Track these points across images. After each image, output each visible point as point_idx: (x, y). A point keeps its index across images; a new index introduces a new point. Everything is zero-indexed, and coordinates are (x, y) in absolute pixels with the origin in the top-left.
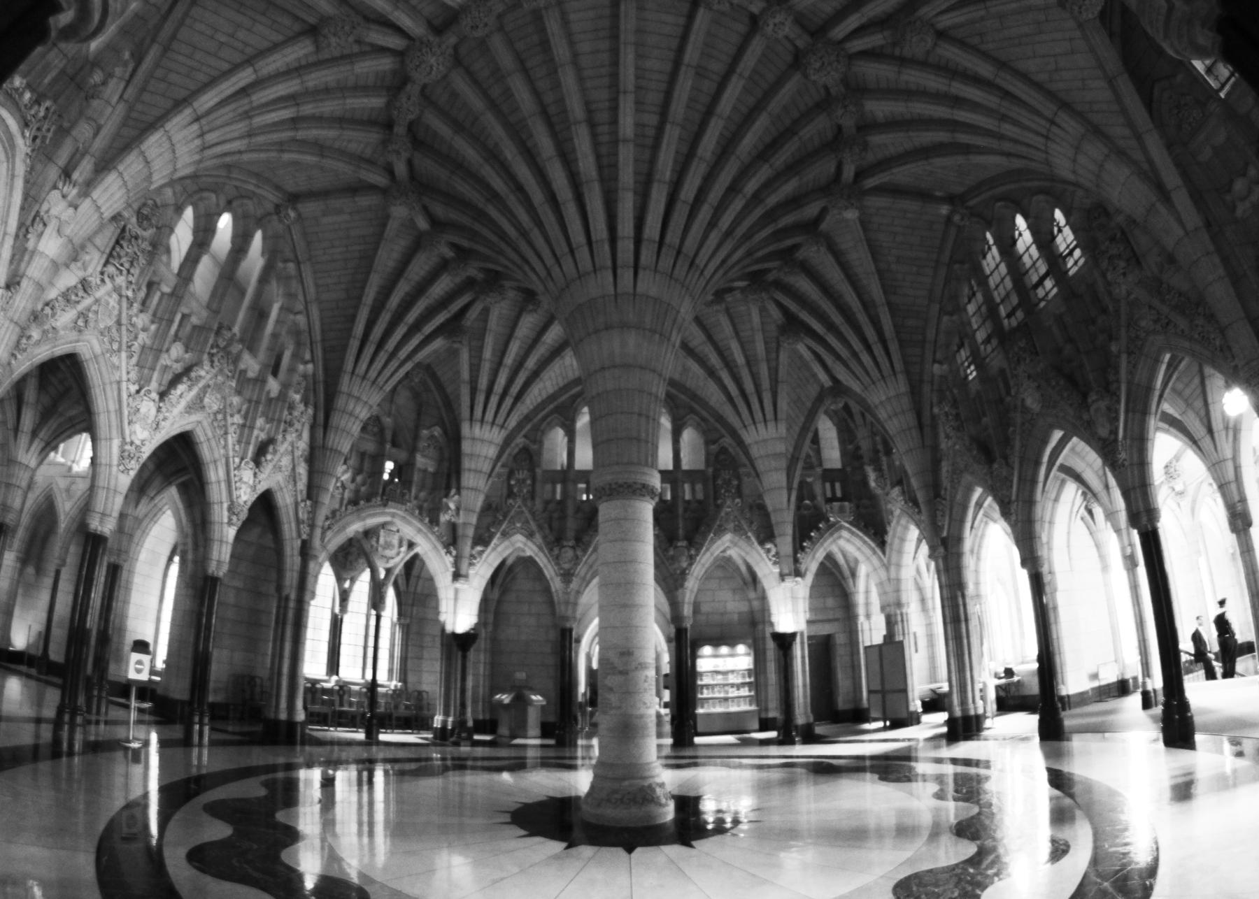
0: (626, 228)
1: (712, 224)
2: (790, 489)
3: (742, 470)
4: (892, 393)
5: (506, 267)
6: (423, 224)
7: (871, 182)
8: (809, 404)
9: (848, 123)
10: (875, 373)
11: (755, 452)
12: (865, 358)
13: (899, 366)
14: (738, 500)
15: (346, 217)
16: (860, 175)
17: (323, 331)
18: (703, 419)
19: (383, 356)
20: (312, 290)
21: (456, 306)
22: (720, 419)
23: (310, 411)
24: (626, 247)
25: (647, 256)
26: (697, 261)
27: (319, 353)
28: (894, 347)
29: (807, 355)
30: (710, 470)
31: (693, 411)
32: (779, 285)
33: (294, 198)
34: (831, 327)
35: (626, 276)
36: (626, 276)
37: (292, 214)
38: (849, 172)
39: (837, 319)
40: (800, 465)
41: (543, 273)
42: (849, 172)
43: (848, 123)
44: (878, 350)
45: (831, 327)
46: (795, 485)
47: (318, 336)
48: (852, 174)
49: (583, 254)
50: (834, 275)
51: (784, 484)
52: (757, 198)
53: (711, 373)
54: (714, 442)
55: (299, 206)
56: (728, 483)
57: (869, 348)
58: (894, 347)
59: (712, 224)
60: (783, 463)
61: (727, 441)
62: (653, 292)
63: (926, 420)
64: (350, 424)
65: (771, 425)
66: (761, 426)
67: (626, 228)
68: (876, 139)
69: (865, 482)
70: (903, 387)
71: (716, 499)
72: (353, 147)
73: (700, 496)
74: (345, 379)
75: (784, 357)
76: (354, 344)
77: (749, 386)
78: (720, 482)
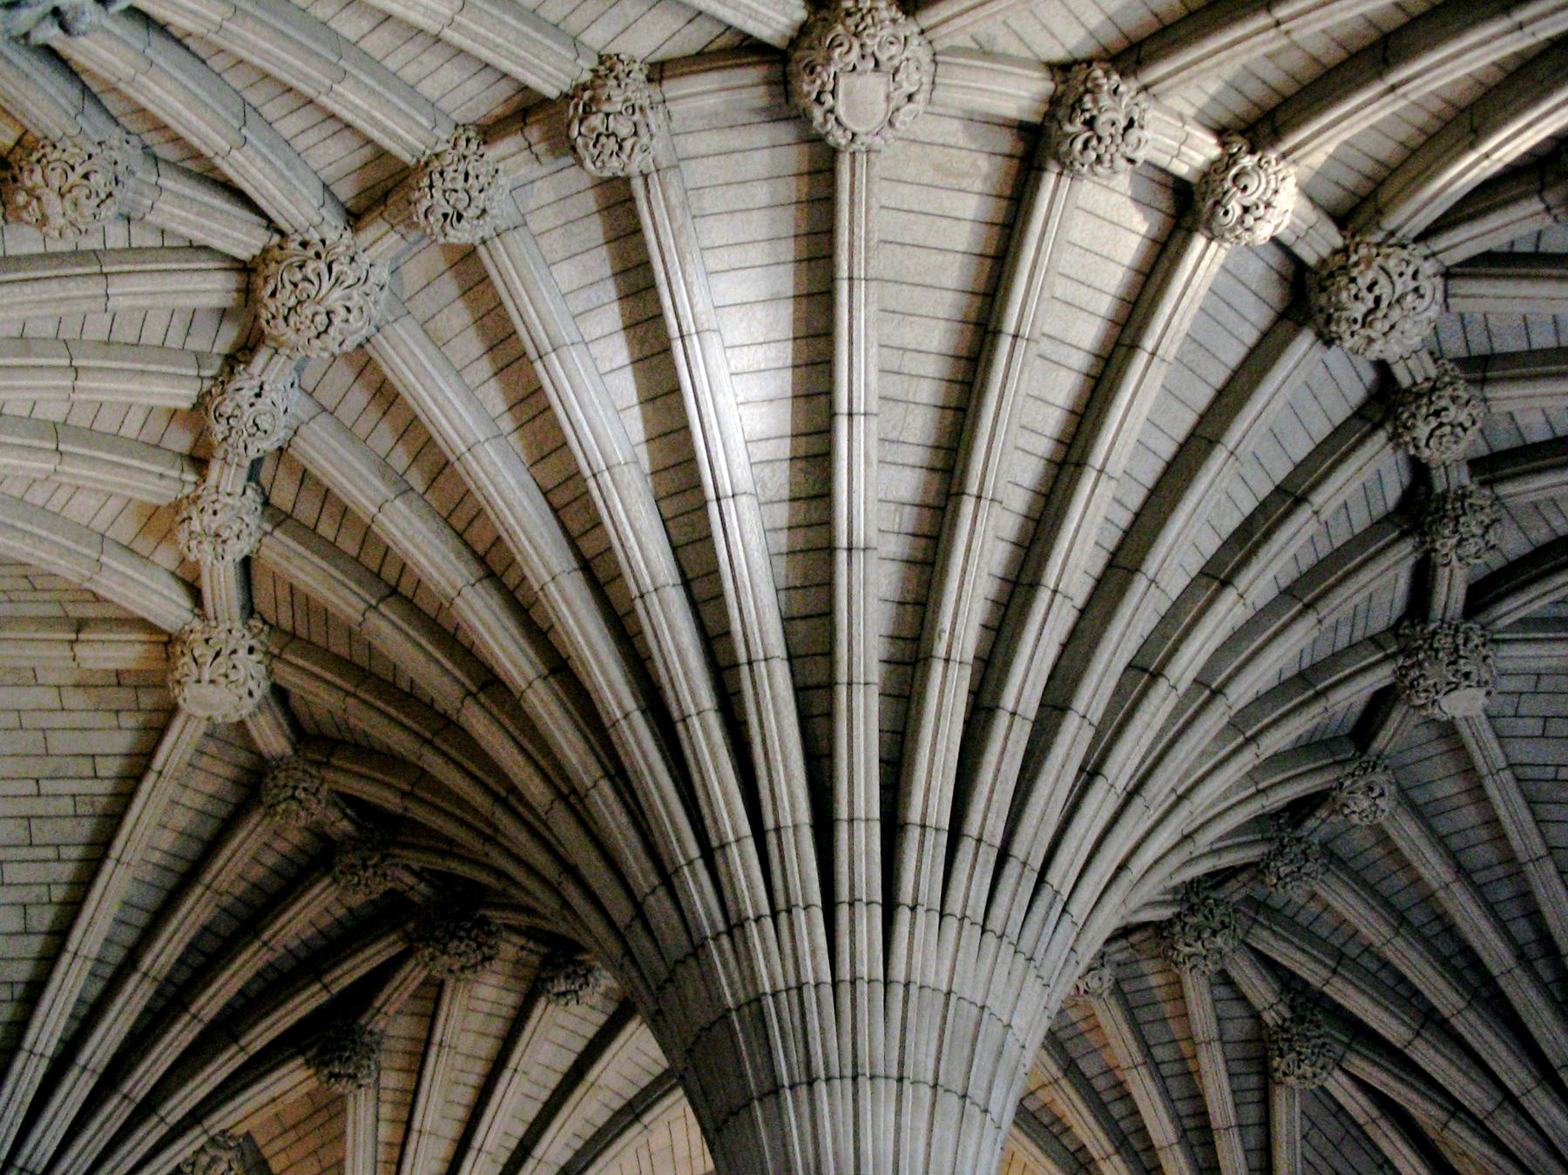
0: (860, 790)
1: (1090, 773)
5: (501, 874)
6: (272, 738)
7: (1512, 609)
9: (1449, 457)
15: (49, 698)
16: (1483, 595)
19: (115, 1112)
21: (347, 974)
24: (861, 844)
26: (1054, 877)
29: (1358, 1106)
34: (1431, 1020)
38: (1450, 592)
39: (1444, 996)
41: (622, 912)
42: (1450, 592)
43: (1449, 457)
45: (1431, 1020)
48: (1459, 592)
49: (743, 861)
52: (1208, 688)
59: (1090, 773)
67: (860, 790)
68: (1521, 491)
75: (1287, 1114)
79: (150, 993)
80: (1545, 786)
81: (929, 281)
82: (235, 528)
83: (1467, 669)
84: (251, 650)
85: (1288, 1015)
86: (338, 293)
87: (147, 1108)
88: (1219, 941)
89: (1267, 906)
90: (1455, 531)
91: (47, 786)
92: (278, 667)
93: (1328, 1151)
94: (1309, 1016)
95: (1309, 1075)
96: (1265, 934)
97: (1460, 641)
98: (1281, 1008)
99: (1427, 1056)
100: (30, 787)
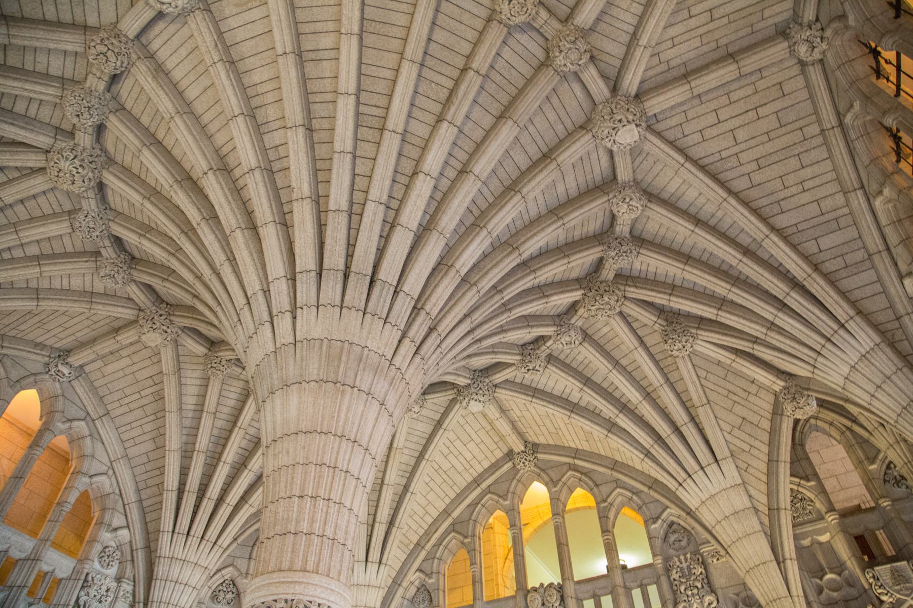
2: (780, 562)
3: (705, 549)
4: (854, 357)
8: (766, 425)
10: (814, 339)
11: (707, 517)
12: (785, 321)
13: (842, 310)
14: (709, 598)
17: (138, 491)
18: (636, 493)
19: (207, 506)
20: (115, 448)
22: (654, 484)
23: (127, 587)
25: (306, 290)
27: (135, 515)
28: (818, 286)
29: (724, 357)
30: (659, 560)
31: (618, 484)
32: (624, 278)
33: (64, 354)
34: (723, 303)
35: (284, 323)
36: (284, 323)
37: (65, 370)
39: (720, 288)
40: (786, 519)
44: (795, 300)
45: (723, 303)
46: (789, 548)
47: (131, 495)
50: (681, 231)
51: (768, 554)
53: (611, 427)
54: (655, 520)
55: (70, 360)
56: (687, 574)
57: (783, 306)
58: (818, 286)
60: (753, 523)
61: (672, 513)
62: (317, 333)
64: (177, 595)
65: (712, 470)
66: (699, 476)
70: (866, 338)
72: (76, 283)
74: (165, 538)
75: (686, 370)
76: (170, 499)
77: (663, 429)
78: (675, 575)
79: (204, 458)
80: (718, 164)
81: (254, 52)
82: (116, 269)
83: (619, 118)
84: (161, 315)
85: (664, 323)
86: (68, 163)
87: (220, 500)
88: (606, 298)
90: (561, 51)
91: (143, 393)
92: (172, 318)
93: (721, 382)
94: (675, 321)
95: (681, 347)
96: (632, 289)
97: (613, 106)
98: (659, 321)
100: (137, 396)
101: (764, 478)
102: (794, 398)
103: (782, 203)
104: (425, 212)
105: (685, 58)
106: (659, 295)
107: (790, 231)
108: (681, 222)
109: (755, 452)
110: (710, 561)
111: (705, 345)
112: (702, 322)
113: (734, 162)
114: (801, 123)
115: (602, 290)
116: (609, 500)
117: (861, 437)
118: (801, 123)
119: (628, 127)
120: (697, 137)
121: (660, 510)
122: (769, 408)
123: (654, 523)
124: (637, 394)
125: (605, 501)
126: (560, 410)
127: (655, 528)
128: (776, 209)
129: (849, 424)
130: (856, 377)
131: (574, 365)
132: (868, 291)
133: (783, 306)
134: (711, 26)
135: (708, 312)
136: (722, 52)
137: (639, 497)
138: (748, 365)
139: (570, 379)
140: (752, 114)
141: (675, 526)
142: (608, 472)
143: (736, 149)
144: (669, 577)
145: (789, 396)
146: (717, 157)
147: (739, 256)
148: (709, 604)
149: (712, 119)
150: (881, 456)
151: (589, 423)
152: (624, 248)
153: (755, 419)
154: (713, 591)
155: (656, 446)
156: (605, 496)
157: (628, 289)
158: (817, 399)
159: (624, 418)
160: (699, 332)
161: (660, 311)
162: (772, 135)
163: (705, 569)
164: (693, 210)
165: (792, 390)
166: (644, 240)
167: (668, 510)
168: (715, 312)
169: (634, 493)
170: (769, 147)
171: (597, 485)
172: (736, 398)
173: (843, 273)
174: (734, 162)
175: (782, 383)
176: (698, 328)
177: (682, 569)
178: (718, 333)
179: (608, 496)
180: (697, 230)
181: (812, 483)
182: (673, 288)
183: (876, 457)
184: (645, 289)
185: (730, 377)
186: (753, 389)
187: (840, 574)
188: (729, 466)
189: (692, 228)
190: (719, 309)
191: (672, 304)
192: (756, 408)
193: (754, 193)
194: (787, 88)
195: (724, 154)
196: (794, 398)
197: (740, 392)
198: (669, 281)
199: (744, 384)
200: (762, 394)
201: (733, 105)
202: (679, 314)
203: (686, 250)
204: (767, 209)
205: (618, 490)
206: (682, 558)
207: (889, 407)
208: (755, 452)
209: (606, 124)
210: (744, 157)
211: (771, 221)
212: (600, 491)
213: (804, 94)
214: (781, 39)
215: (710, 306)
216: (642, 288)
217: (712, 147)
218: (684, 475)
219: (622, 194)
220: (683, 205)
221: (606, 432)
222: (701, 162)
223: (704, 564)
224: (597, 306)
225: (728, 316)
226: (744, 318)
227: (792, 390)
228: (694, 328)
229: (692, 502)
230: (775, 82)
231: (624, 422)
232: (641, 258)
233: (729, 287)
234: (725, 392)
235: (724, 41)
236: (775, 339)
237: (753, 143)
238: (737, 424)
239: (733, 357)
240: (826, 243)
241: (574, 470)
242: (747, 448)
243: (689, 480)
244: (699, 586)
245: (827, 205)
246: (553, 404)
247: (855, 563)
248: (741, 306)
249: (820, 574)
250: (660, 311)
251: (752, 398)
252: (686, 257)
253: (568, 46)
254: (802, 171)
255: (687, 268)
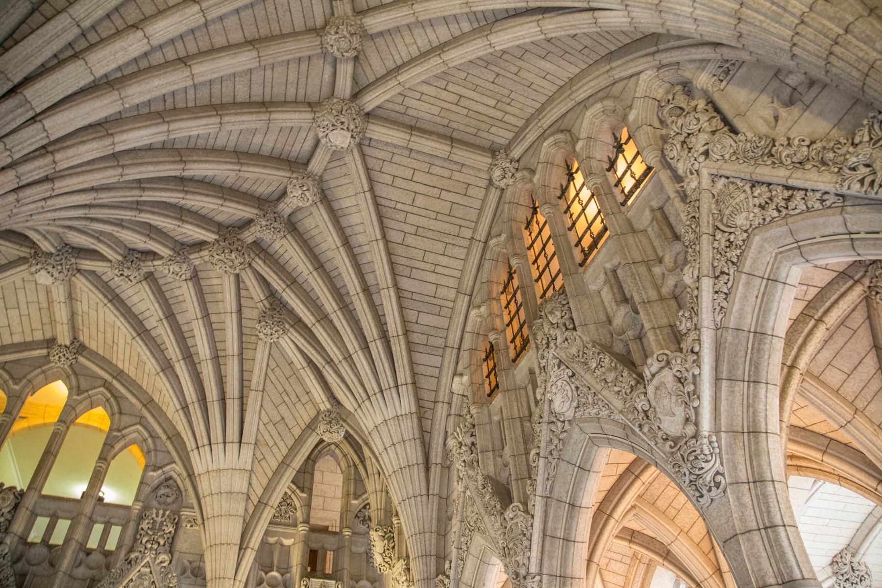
3: (185, 513)
4: (391, 414)
8: (297, 432)
10: (371, 385)
11: (204, 486)
13: (404, 375)
14: (164, 557)
18: (154, 436)
22: (175, 437)
28: (399, 347)
29: (298, 361)
30: (138, 506)
31: (142, 421)
32: (259, 248)
34: (324, 318)
39: (330, 305)
40: (267, 515)
44: (377, 348)
46: (255, 541)
50: (328, 241)
53: (167, 367)
54: (156, 468)
56: (156, 528)
57: (365, 347)
58: (399, 347)
60: (239, 507)
61: (176, 469)
63: (436, 457)
65: (232, 448)
66: (218, 449)
69: (369, 555)
70: (406, 404)
71: (131, 551)
73: (111, 545)
75: (261, 355)
78: (145, 525)
80: (390, 210)
83: (343, 120)
85: (268, 306)
88: (233, 256)
89: (266, 252)
94: (278, 309)
95: (269, 332)
96: (260, 262)
97: (345, 108)
98: (265, 302)
99: (320, 332)
101: (270, 474)
102: (330, 422)
103: (414, 270)
104: (120, 68)
105: (421, 115)
106: (278, 281)
107: (406, 294)
108: (334, 234)
109: (275, 450)
110: (184, 524)
111: (289, 343)
112: (298, 323)
113: (401, 216)
114: (463, 223)
115: (235, 246)
116: (124, 432)
117: (360, 476)
118: (463, 223)
119: (345, 133)
120: (388, 179)
121: (166, 461)
122: (307, 420)
123: (154, 470)
124: (208, 352)
125: (119, 431)
126: (128, 326)
127: (152, 476)
128: (406, 272)
129: (357, 461)
130: (383, 429)
131: (168, 295)
132: (429, 371)
133: (365, 347)
134: (453, 108)
135: (308, 318)
136: (447, 132)
137: (154, 442)
138: (312, 377)
139: (157, 305)
140: (436, 192)
141: (171, 482)
142: (138, 405)
143: (409, 209)
144: (139, 524)
145: (328, 419)
146: (392, 204)
147: (359, 290)
148: (161, 562)
149: (408, 174)
150: (364, 497)
151: (148, 353)
152: (276, 225)
153: (291, 423)
154: (171, 552)
155: (196, 405)
156: (121, 427)
157: (257, 259)
158: (347, 432)
159: (183, 366)
160: (291, 330)
161: (272, 294)
162: (440, 217)
163: (176, 530)
164: (348, 231)
165: (333, 416)
166: (296, 229)
167: (174, 465)
168: (314, 321)
169: (151, 436)
170: (432, 224)
171: (120, 413)
172: (286, 399)
173: (421, 348)
174: (401, 216)
175: (329, 406)
176: (292, 326)
177: (155, 522)
178: (305, 339)
179: (125, 428)
180: (341, 249)
181: (304, 495)
182: (293, 282)
183: (360, 496)
184: (271, 268)
185: (293, 380)
186: (305, 398)
187: (282, 575)
188: (247, 452)
189: (339, 244)
190: (318, 321)
191: (284, 294)
192: (297, 415)
193: (399, 250)
194: (471, 192)
195: (399, 206)
196: (330, 422)
197: (293, 397)
198: (294, 275)
199: (300, 391)
200: (309, 406)
201: (428, 175)
202: (284, 305)
203: (323, 258)
204: (401, 268)
205: (138, 427)
206: (161, 512)
207: (391, 463)
208: (275, 450)
209: (329, 117)
210: (411, 219)
211: (398, 278)
212: (120, 419)
213: (477, 204)
214: (489, 155)
215: (313, 315)
216: (268, 266)
217: (394, 194)
218: (206, 441)
219: (304, 181)
220: (344, 222)
221: (159, 370)
222: (379, 199)
223: (177, 526)
224: (222, 257)
225: (321, 330)
226: (332, 340)
227: (333, 416)
228: (289, 323)
229: (199, 466)
230: (466, 181)
231: (181, 369)
232: (284, 241)
233: (336, 308)
234: (281, 390)
235: (454, 125)
236: (345, 369)
237: (423, 212)
238: (275, 421)
239: (305, 364)
240: (425, 319)
241: (107, 389)
242: (271, 443)
243: (207, 448)
244: (162, 542)
245: (442, 292)
246: (126, 319)
247: (299, 570)
248: (336, 328)
249: (268, 569)
250: (272, 294)
251: (299, 405)
252: (319, 264)
253: (345, 33)
254: (442, 257)
255: (315, 273)
